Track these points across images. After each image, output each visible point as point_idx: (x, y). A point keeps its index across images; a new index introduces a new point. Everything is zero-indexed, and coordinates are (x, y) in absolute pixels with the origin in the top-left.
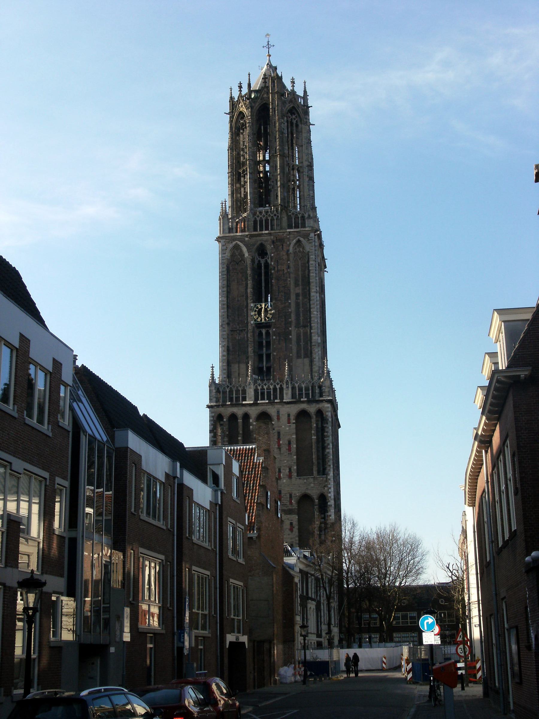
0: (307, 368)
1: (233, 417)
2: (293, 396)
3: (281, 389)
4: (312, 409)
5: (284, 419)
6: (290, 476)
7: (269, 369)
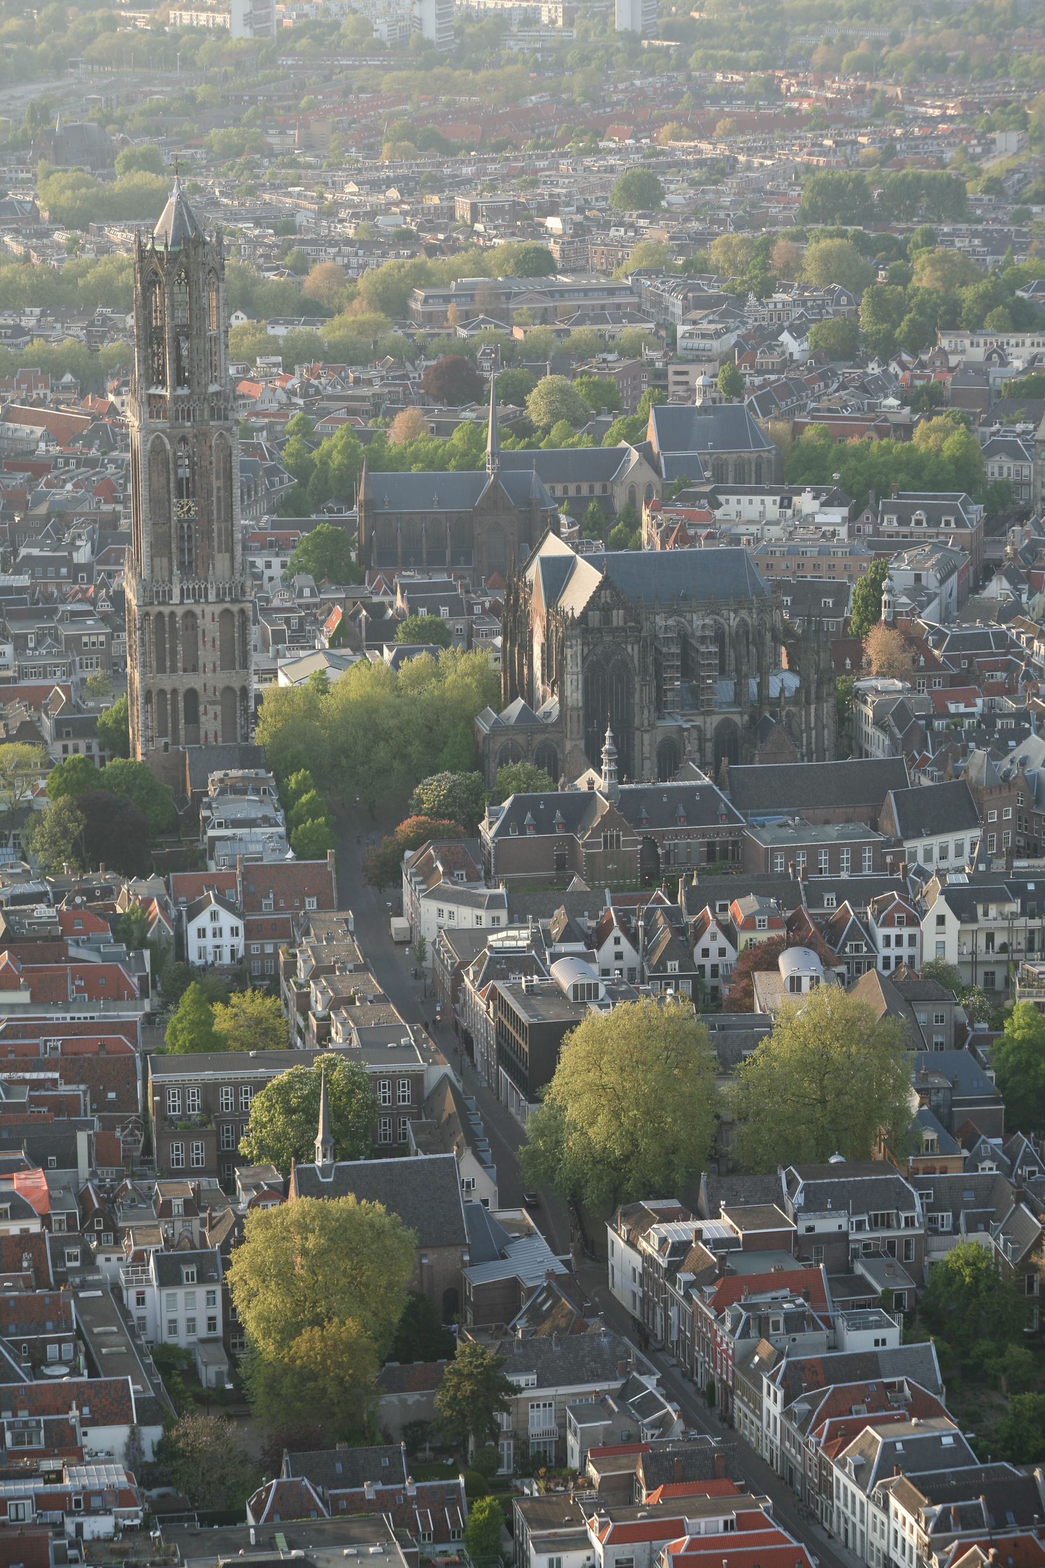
0: (227, 563)
1: (160, 614)
2: (218, 595)
3: (206, 588)
4: (235, 608)
5: (208, 617)
6: (214, 670)
7: (190, 563)
